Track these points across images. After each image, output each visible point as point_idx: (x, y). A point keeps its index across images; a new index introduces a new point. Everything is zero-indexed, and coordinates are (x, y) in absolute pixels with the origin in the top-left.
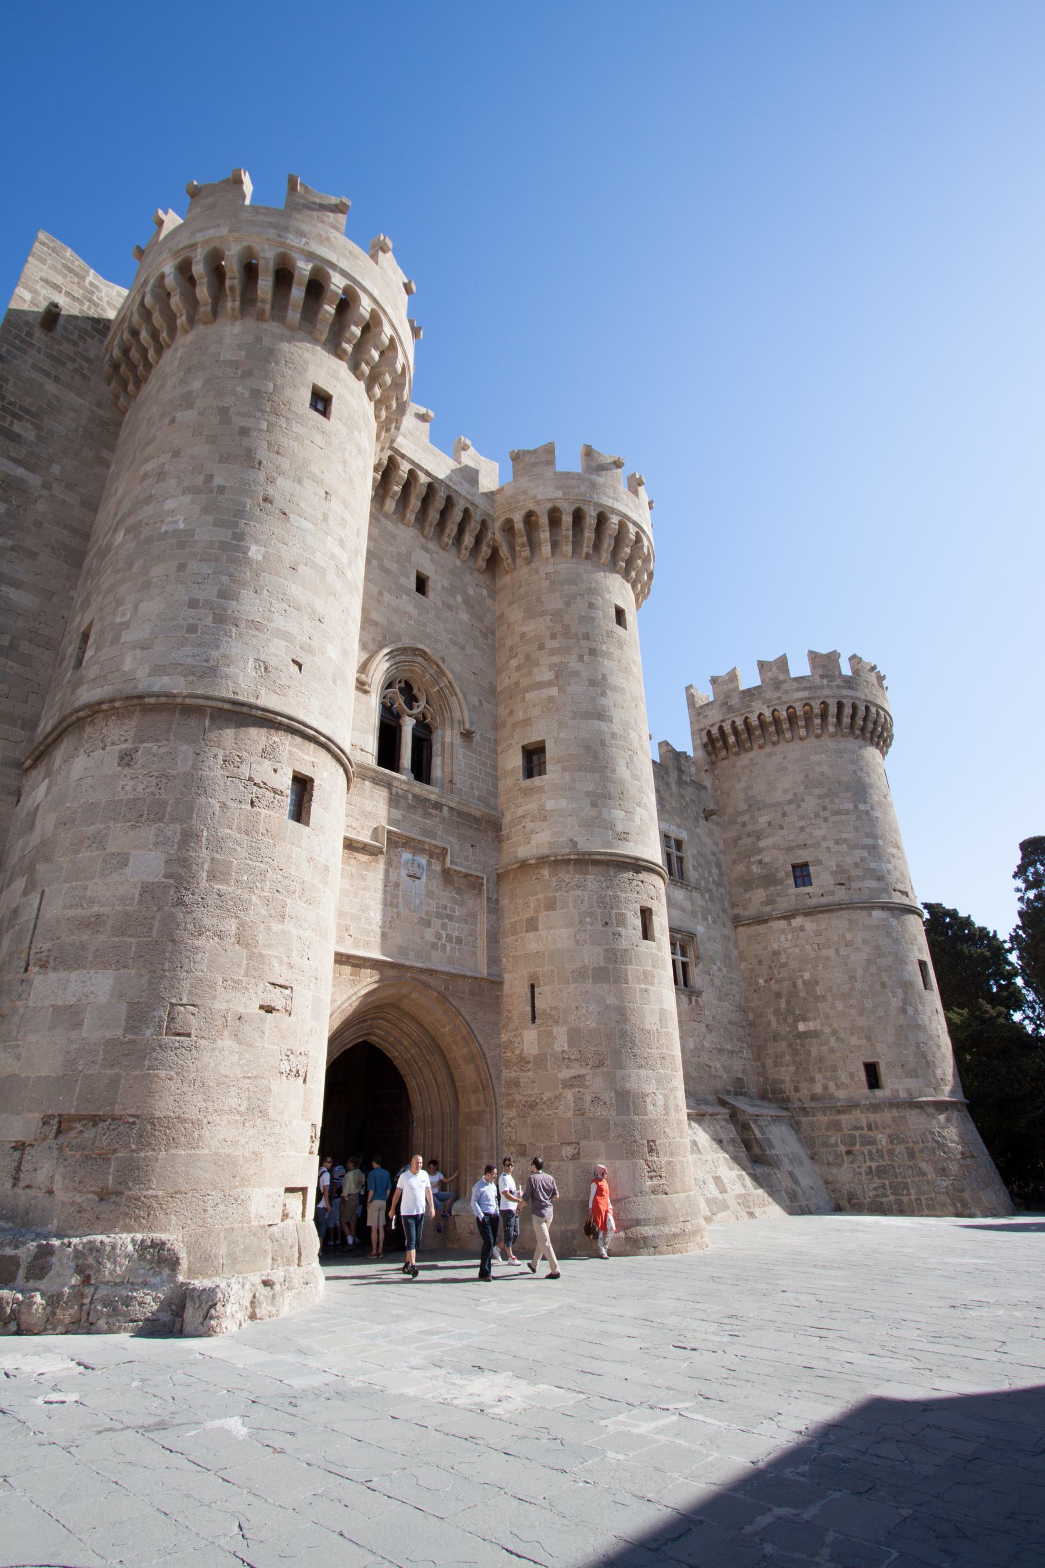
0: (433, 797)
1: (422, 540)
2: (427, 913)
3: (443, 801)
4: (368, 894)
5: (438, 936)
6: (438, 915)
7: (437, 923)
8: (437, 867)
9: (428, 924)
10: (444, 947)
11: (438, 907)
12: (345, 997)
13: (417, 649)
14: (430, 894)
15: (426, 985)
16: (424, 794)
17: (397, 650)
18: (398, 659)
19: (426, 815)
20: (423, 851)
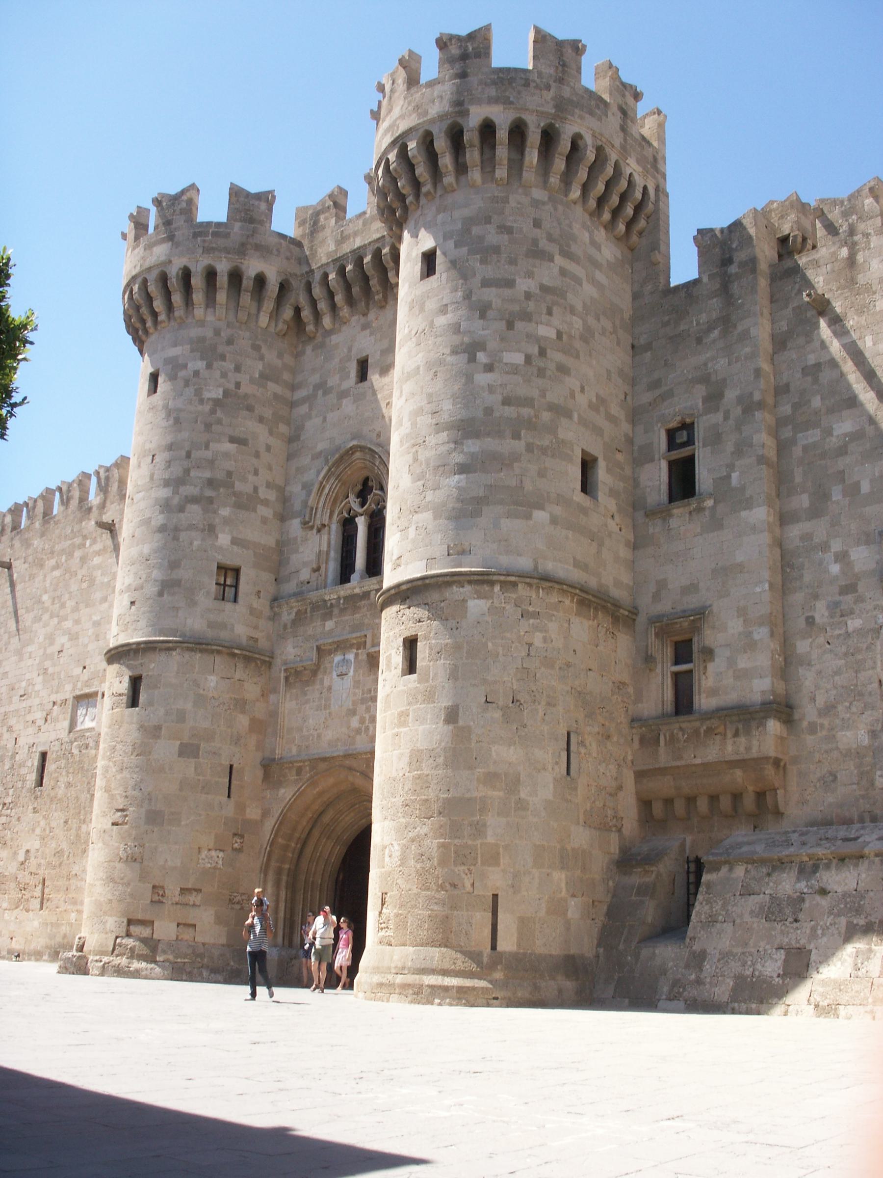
0: (357, 591)
1: (363, 320)
2: (354, 703)
3: (366, 589)
4: (308, 706)
5: (362, 721)
6: (363, 701)
7: (361, 708)
8: (363, 657)
9: (353, 712)
10: (367, 728)
11: (363, 694)
12: (292, 794)
13: (351, 448)
14: (357, 684)
15: (350, 769)
16: (349, 592)
17: (333, 465)
18: (337, 473)
19: (356, 609)
20: (352, 646)
